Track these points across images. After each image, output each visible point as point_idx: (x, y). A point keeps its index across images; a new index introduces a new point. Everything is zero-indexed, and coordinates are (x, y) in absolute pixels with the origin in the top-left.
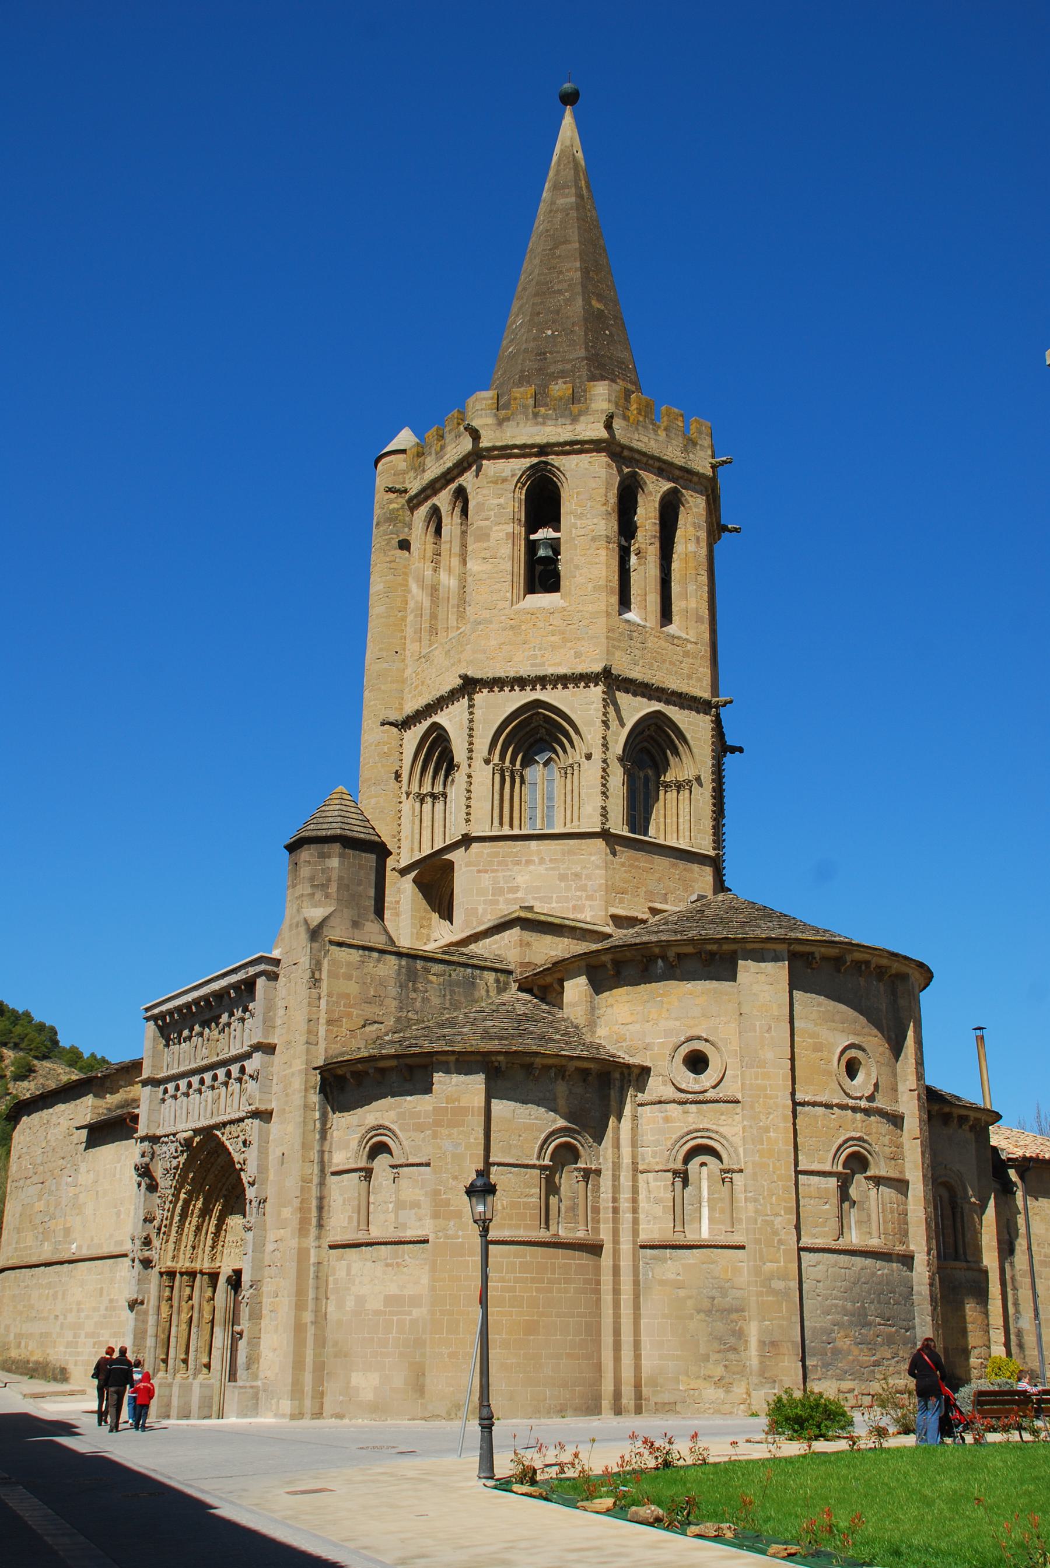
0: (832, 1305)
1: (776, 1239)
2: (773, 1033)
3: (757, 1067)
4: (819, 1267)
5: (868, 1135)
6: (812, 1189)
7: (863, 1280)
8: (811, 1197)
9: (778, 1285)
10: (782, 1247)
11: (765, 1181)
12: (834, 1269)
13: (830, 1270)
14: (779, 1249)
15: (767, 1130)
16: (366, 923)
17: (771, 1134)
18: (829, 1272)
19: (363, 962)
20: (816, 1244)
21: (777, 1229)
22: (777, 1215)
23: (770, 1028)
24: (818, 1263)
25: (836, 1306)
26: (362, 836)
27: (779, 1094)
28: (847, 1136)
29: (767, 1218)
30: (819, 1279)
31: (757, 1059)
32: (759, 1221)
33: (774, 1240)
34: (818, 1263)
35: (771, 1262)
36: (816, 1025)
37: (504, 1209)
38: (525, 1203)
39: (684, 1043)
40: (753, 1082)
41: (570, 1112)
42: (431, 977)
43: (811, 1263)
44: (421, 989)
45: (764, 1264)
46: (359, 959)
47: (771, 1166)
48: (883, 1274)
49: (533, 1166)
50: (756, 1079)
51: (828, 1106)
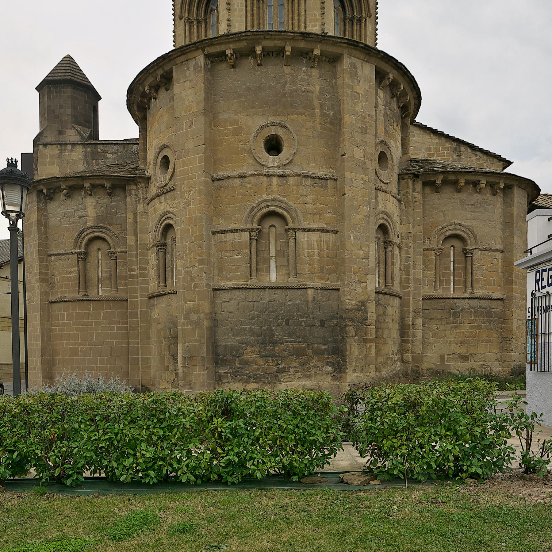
0: (241, 329)
2: (193, 127)
4: (232, 302)
7: (271, 309)
9: (194, 317)
14: (195, 291)
16: (67, 130)
17: (191, 206)
19: (62, 153)
20: (227, 285)
22: (194, 266)
25: (244, 330)
26: (62, 78)
28: (261, 199)
30: (231, 310)
34: (231, 299)
37: (58, 282)
38: (69, 277)
39: (160, 152)
42: (108, 156)
43: (225, 300)
44: (102, 163)
45: (186, 303)
46: (58, 152)
48: (293, 305)
49: (72, 253)
51: (241, 177)
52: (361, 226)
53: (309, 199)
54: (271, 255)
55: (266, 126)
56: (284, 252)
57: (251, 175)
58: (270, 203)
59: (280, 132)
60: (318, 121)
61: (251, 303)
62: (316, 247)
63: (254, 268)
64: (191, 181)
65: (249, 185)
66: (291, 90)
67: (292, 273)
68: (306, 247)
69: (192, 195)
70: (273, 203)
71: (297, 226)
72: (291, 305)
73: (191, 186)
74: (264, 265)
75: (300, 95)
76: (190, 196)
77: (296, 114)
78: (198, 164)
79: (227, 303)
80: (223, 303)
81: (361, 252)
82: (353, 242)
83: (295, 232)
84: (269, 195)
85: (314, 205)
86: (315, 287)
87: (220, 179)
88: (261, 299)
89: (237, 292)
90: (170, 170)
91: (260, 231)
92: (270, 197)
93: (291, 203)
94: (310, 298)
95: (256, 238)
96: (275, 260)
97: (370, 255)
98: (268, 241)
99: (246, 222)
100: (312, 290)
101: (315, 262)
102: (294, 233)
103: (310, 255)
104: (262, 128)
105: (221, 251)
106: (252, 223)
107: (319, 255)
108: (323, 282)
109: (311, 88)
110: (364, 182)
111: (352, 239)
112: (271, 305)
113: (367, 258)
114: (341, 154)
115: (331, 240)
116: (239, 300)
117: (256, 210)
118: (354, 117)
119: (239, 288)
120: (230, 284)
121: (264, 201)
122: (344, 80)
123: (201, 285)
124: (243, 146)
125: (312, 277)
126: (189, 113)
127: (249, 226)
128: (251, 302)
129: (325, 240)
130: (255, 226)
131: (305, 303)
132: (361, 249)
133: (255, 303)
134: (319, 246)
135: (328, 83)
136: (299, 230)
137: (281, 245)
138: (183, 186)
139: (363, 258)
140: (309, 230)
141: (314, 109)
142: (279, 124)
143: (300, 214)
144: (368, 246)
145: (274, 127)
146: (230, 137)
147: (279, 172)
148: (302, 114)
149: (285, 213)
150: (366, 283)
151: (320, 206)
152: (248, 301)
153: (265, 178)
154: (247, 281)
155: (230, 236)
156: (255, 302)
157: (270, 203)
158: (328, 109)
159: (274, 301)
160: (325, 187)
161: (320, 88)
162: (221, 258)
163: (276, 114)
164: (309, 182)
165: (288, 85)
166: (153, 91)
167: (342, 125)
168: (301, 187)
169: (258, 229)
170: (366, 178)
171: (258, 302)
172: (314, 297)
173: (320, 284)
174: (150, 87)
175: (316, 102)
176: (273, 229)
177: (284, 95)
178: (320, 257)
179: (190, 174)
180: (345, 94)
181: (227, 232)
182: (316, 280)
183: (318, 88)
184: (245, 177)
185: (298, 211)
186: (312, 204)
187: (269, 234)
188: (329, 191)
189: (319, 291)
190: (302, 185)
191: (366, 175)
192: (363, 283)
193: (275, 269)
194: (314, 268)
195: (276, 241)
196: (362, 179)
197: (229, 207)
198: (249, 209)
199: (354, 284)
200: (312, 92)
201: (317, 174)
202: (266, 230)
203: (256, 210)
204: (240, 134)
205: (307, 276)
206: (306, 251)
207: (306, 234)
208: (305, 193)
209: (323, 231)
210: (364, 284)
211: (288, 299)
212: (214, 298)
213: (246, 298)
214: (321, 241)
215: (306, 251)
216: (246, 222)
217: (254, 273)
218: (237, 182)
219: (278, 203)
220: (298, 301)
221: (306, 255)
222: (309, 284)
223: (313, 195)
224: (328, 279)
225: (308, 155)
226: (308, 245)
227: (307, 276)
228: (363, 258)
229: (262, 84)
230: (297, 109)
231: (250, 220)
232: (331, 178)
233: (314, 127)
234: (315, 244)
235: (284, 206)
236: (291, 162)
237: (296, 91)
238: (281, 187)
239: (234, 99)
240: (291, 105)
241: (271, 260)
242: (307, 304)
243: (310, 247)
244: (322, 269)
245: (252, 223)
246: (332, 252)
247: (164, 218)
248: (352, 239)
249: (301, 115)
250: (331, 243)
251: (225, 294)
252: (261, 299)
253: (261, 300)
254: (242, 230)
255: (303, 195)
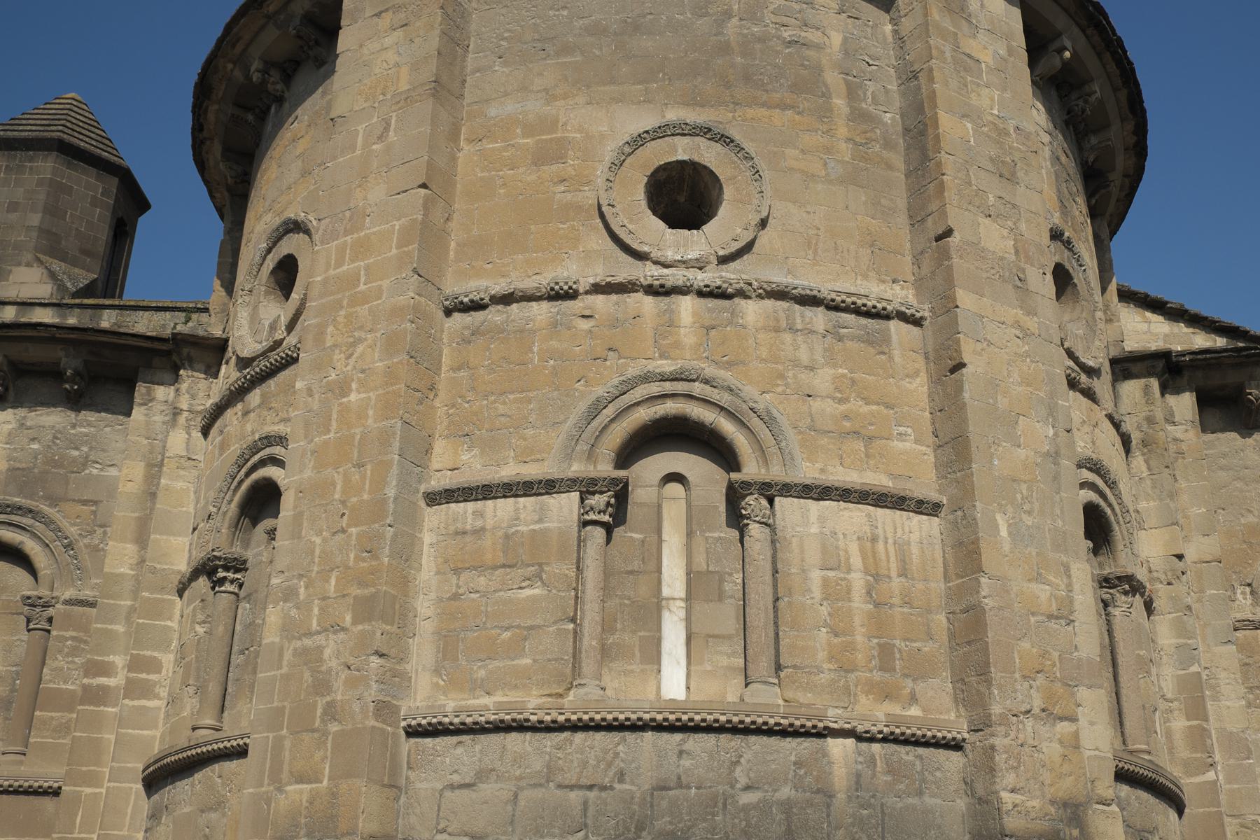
1: (321, 703)
2: (392, 136)
3: (346, 233)
4: (488, 789)
5: (729, 365)
6: (487, 541)
8: (479, 568)
10: (334, 727)
11: (319, 533)
12: (538, 793)
13: (523, 796)
15: (342, 388)
17: (353, 397)
18: (522, 803)
21: (330, 670)
23: (386, 129)
24: (483, 775)
27: (385, 283)
28: (632, 371)
29: (307, 642)
31: (348, 214)
32: (288, 656)
33: (315, 705)
34: (483, 775)
35: (300, 780)
36: (550, 96)
40: (332, 272)
41: (12, 470)
43: (456, 778)
47: (339, 487)
48: (764, 807)
50: (339, 263)
52: (1030, 489)
53: (823, 380)
54: (666, 592)
55: (661, 132)
56: (721, 581)
57: (597, 289)
58: (668, 387)
59: (709, 154)
60: (842, 131)
61: (574, 795)
62: (857, 561)
63: (589, 641)
64: (363, 311)
65: (585, 325)
66: (745, 36)
67: (763, 665)
68: (813, 555)
69: (361, 356)
70: (680, 387)
71: (776, 473)
72: (755, 806)
73: (361, 328)
74: (634, 632)
75: (778, 52)
76: (352, 361)
77: (765, 105)
78: (394, 251)
79: (466, 792)
80: (448, 794)
81: (1042, 592)
82: (1007, 547)
83: (771, 501)
84: (662, 356)
85: (841, 401)
86: (860, 729)
87: (477, 306)
88: (621, 776)
89: (514, 740)
90: (295, 296)
91: (622, 494)
92: (667, 366)
93: (750, 391)
94: (840, 777)
95: (606, 518)
96: (682, 613)
97: (1077, 606)
98: (654, 537)
99: (569, 456)
100: (850, 742)
101: (857, 621)
102: (764, 502)
103: (835, 593)
104: (639, 141)
105: (457, 571)
106: (591, 456)
107: (869, 593)
108: (895, 709)
109: (813, 36)
110: (1026, 335)
111: (1004, 532)
112: (664, 804)
113: (1064, 615)
114: (932, 234)
115: (915, 537)
116: (520, 778)
117: (609, 412)
118: (969, 125)
119: (521, 727)
120: (487, 705)
121: (646, 378)
122: (926, 15)
123: (356, 707)
124: (569, 196)
125: (847, 689)
126: (381, 98)
127: (577, 469)
128: (572, 787)
129: (889, 535)
130: (605, 468)
131: (818, 798)
132: (1039, 578)
133: (592, 795)
134: (870, 556)
135: (869, 30)
136: (787, 489)
137: (707, 553)
138: (330, 329)
139: (1050, 617)
140: (823, 493)
141: (827, 95)
142: (704, 131)
143: (790, 433)
144: (1067, 569)
145: (686, 140)
146: (521, 170)
147: (701, 278)
148: (784, 107)
149: (727, 427)
150: (1073, 719)
151: (865, 409)
152: (560, 786)
153: (649, 300)
154: (561, 696)
155: (502, 508)
156: (590, 787)
157: (668, 387)
158: (875, 101)
159: (680, 785)
160: (880, 343)
161: (845, 40)
162: (455, 597)
163: (692, 101)
164: (819, 318)
165: (735, 21)
166: (275, 76)
167: (930, 146)
168: (787, 337)
169: (614, 481)
170: (1032, 324)
171: (604, 788)
172: (858, 775)
173: (881, 715)
174: (268, 65)
175: (833, 78)
176: (675, 489)
177: (725, 49)
178: (877, 605)
179: (362, 287)
180: (934, 52)
181: (485, 492)
182: (863, 699)
183: (836, 39)
184: (571, 295)
185: (784, 422)
186: (834, 398)
187: (659, 507)
188: (897, 359)
189: (876, 747)
190: (792, 329)
191: (1031, 312)
192: (1062, 719)
193: (681, 651)
194: (850, 647)
195: (690, 534)
196: (1017, 325)
197: (504, 403)
198: (582, 406)
199: (1029, 723)
200: (819, 47)
201: (849, 294)
202: (641, 495)
203: (609, 412)
204: (560, 158)
205: (824, 678)
206: (816, 575)
207: (814, 508)
208: (803, 355)
209: (880, 499)
210: (1064, 727)
211: (743, 781)
212: (409, 768)
213: (550, 770)
214: (874, 540)
215: (816, 575)
216: (569, 456)
217: (588, 666)
218: (541, 311)
219: (697, 388)
220: (786, 792)
221: (817, 593)
222: (836, 716)
223: (835, 366)
224: (913, 699)
225: (812, 232)
226: (824, 550)
227: (824, 678)
228: (1050, 617)
229: (644, 17)
230: (767, 91)
231: (583, 447)
232: (902, 317)
233: (828, 150)
234: (854, 548)
235: (725, 399)
236: (748, 248)
237: (761, 40)
238: (713, 333)
239: (545, 59)
240: (747, 78)
241: (666, 615)
242: (828, 806)
243: (833, 560)
244: (886, 656)
245: (591, 456)
246: (920, 586)
247: (250, 464)
248: (1004, 532)
249: (783, 110)
250: (915, 550)
251: (460, 750)
252: (621, 776)
253: (621, 781)
254: (550, 486)
255: (796, 363)
